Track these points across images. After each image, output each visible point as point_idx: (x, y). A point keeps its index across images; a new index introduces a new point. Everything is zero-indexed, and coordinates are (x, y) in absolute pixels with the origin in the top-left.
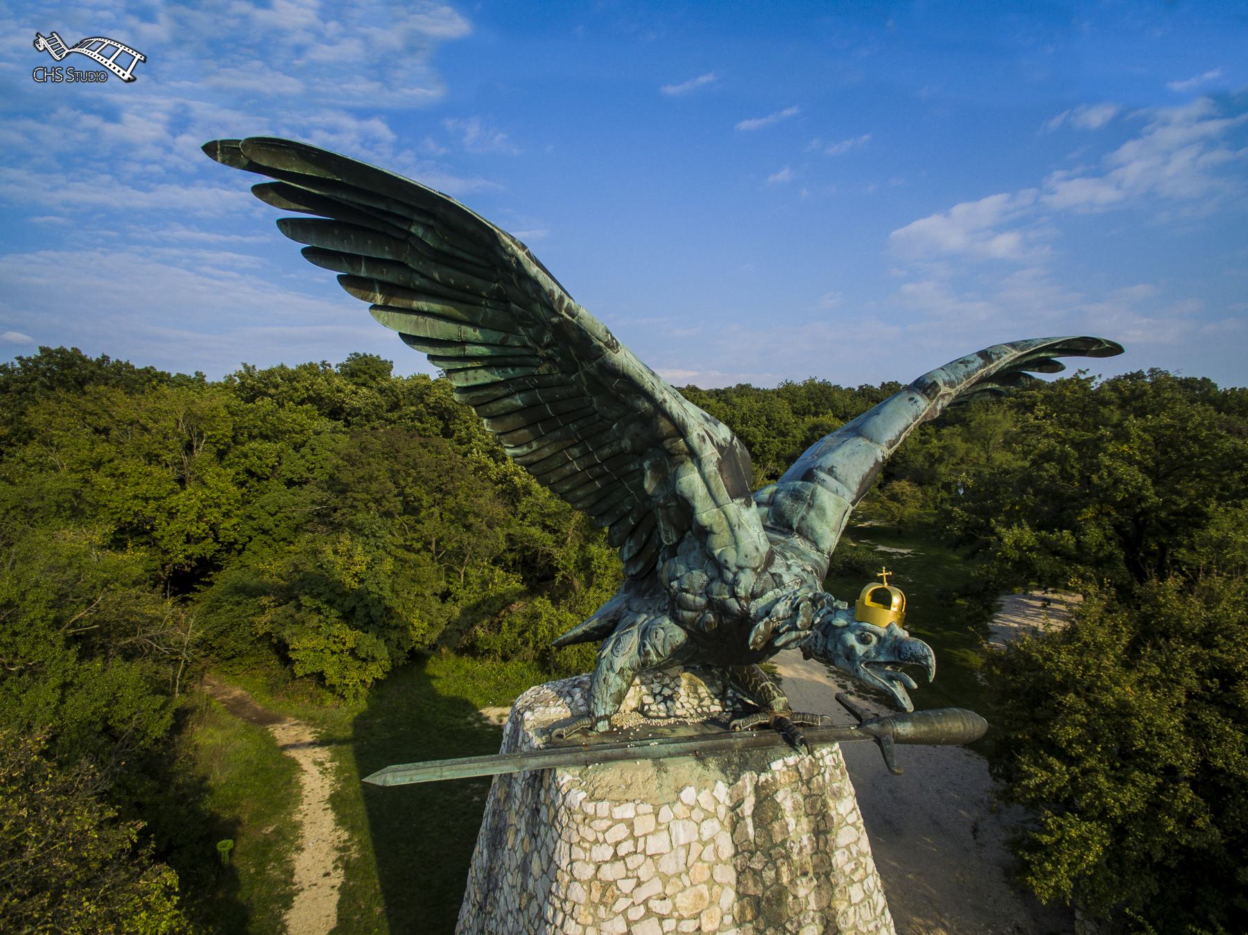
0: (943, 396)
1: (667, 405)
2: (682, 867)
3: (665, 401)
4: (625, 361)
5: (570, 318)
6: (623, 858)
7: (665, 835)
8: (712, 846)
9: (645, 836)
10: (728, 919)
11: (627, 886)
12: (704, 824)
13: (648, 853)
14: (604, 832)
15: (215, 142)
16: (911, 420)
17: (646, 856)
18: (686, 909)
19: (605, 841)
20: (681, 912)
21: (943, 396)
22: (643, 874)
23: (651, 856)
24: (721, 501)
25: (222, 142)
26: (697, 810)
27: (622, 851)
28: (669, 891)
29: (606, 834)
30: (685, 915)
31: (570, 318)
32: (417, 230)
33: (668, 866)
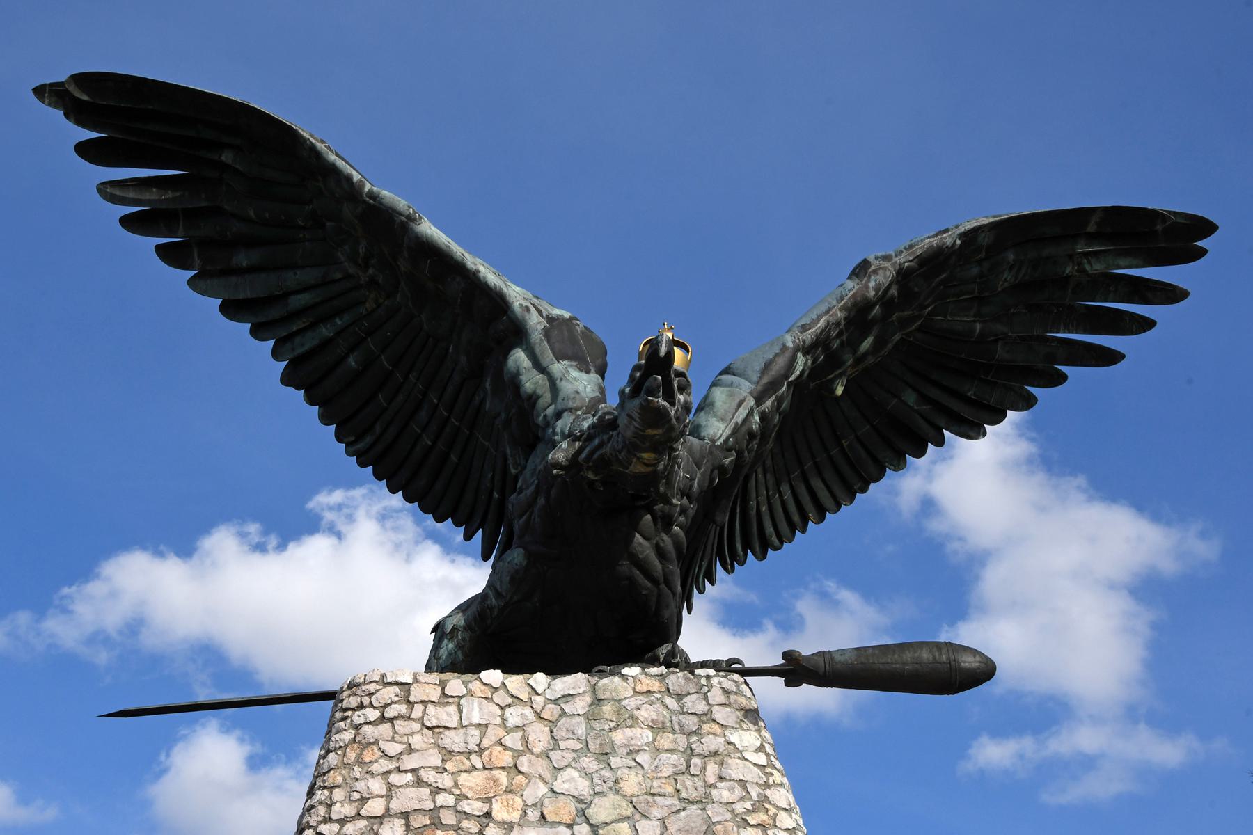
0: (875, 272)
1: (481, 275)
2: (472, 746)
3: (478, 271)
4: (429, 232)
5: (372, 202)
6: (391, 720)
7: (452, 709)
8: (520, 734)
9: (423, 702)
10: (533, 815)
11: (393, 749)
12: (509, 711)
13: (428, 724)
14: (371, 695)
15: (45, 85)
16: (834, 302)
17: (423, 725)
18: (471, 788)
19: (371, 705)
20: (464, 791)
21: (875, 272)
22: (416, 741)
23: (428, 728)
24: (544, 363)
25: (51, 85)
26: (501, 692)
27: (390, 713)
28: (448, 766)
29: (373, 698)
30: (470, 795)
31: (372, 202)
32: (227, 157)
33: (453, 740)
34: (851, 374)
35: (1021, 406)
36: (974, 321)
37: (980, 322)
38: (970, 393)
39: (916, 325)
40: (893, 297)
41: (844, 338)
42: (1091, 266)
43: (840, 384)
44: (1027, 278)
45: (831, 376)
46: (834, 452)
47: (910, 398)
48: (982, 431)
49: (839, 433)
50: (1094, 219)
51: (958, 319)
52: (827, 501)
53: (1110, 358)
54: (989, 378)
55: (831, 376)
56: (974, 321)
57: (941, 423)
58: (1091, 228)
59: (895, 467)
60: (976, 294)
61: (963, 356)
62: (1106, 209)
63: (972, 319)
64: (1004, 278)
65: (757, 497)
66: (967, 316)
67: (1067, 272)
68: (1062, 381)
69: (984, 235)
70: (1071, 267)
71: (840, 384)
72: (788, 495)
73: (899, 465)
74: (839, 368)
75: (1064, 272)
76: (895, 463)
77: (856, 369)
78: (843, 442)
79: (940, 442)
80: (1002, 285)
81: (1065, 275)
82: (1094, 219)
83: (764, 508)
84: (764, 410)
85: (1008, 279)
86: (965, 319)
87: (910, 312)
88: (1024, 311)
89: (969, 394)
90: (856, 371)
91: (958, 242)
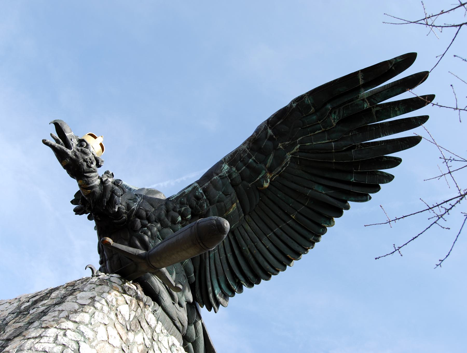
34: (272, 178)
35: (385, 181)
36: (331, 142)
37: (334, 142)
38: (352, 180)
39: (296, 148)
40: (271, 136)
41: (253, 158)
42: (377, 101)
43: (265, 182)
44: (345, 115)
45: (258, 178)
46: (290, 222)
47: (320, 189)
48: (368, 197)
49: (286, 212)
50: (360, 77)
51: (320, 142)
52: (299, 249)
53: (415, 141)
54: (359, 171)
55: (258, 178)
56: (331, 142)
57: (344, 198)
58: (361, 82)
59: (328, 225)
60: (323, 129)
61: (334, 161)
62: (363, 71)
63: (328, 141)
64: (333, 117)
65: (247, 246)
66: (324, 140)
67: (365, 106)
68: (400, 162)
69: (307, 99)
70: (366, 104)
71: (265, 182)
72: (269, 245)
73: (330, 223)
74: (260, 174)
75: (364, 107)
76: (328, 223)
77: (273, 175)
78: (291, 216)
79: (348, 208)
80: (334, 121)
81: (365, 109)
82: (360, 77)
83: (255, 252)
84: (204, 187)
85: (335, 118)
86: (324, 142)
87: (288, 142)
88: (357, 133)
89: (352, 180)
90: (274, 176)
91: (294, 105)
